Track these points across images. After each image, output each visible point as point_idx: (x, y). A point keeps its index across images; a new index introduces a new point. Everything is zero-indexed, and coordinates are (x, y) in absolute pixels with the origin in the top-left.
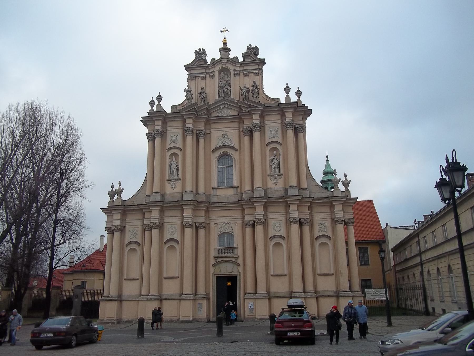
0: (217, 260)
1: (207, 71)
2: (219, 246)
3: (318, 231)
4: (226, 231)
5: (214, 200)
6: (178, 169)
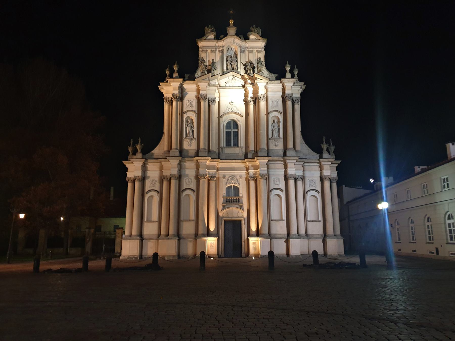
3: (309, 187)
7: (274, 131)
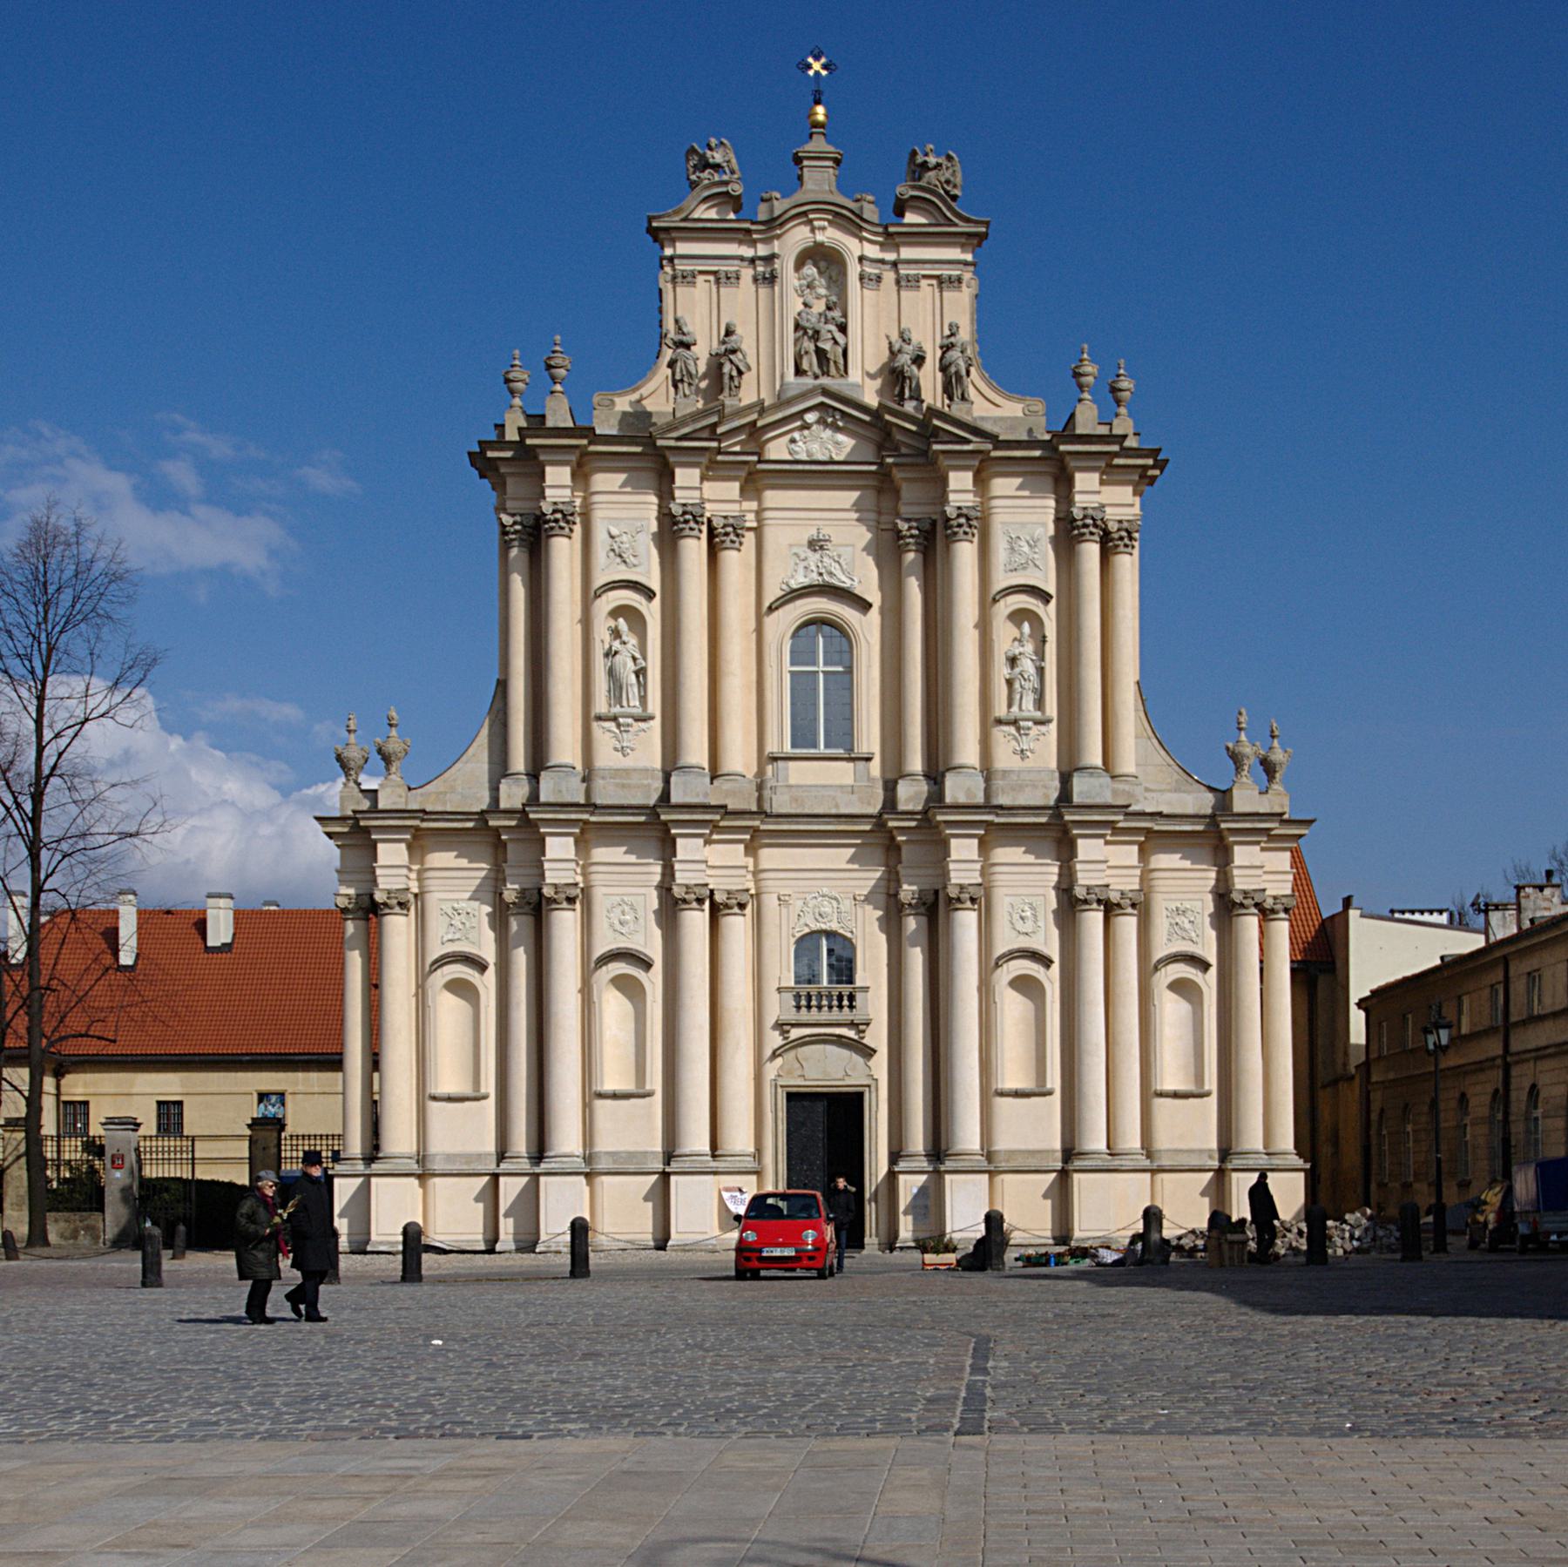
0: (788, 1032)
1: (747, 252)
2: (797, 982)
4: (824, 927)
5: (780, 803)
6: (641, 673)
7: (1017, 686)
